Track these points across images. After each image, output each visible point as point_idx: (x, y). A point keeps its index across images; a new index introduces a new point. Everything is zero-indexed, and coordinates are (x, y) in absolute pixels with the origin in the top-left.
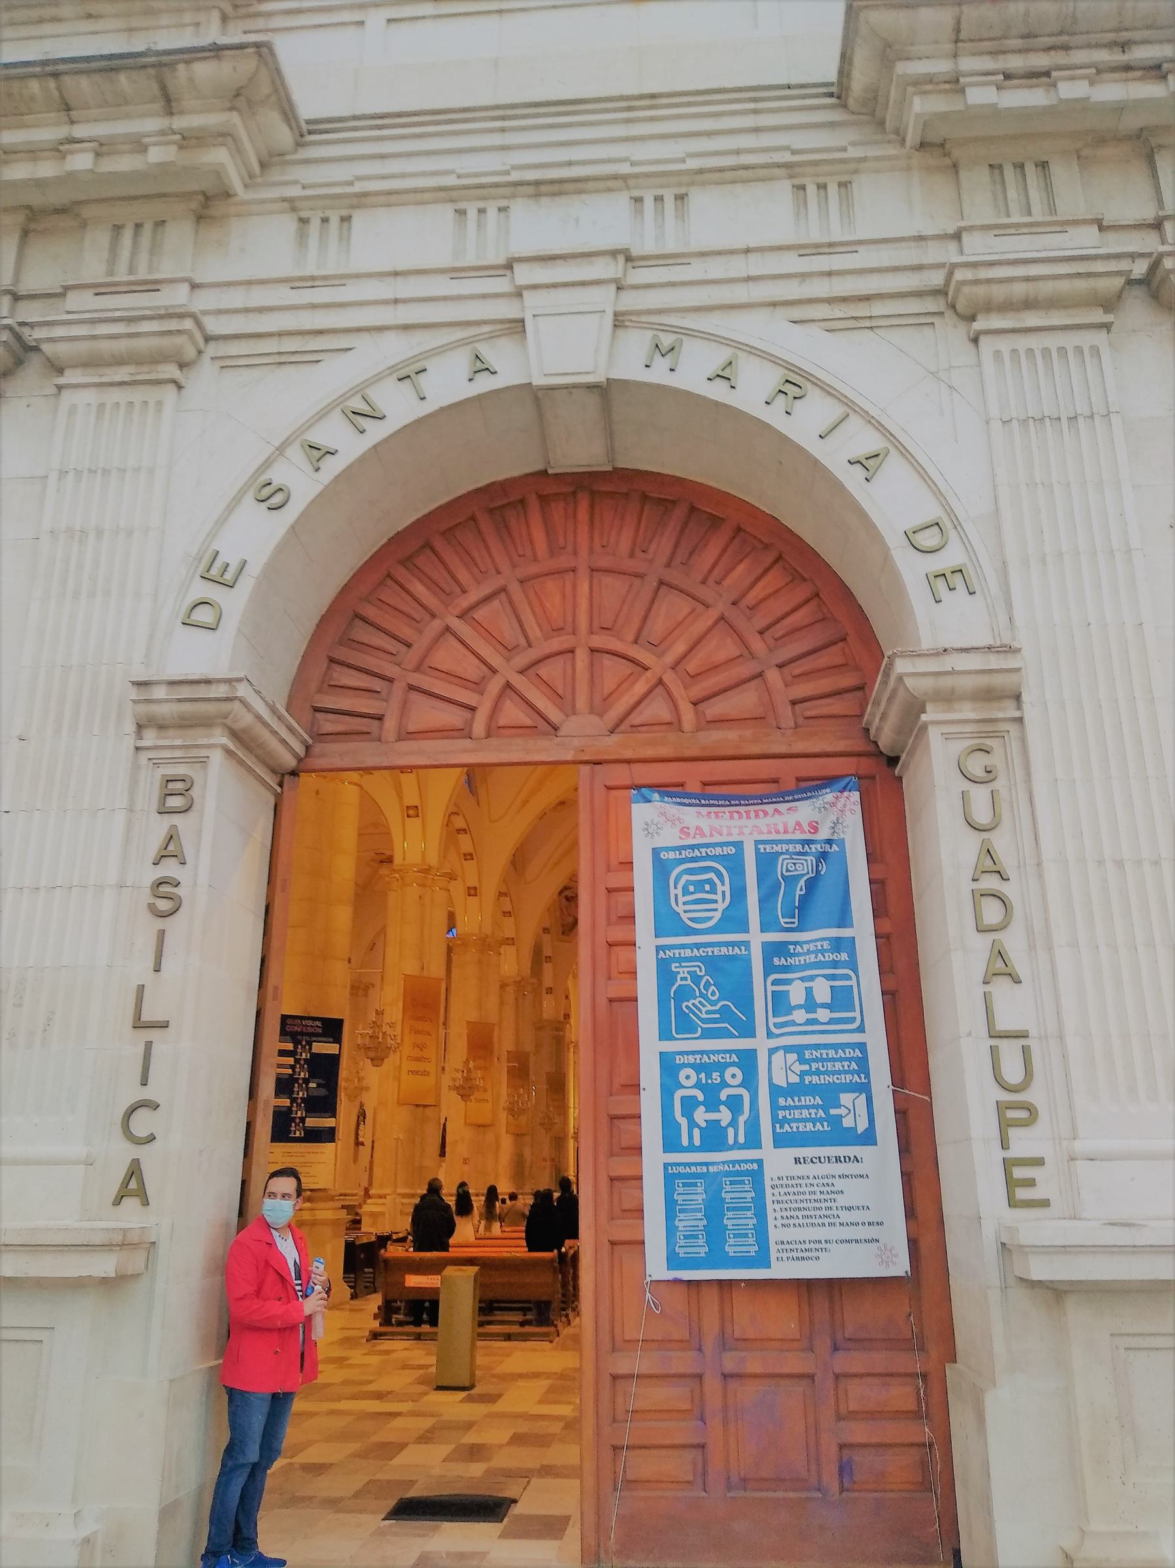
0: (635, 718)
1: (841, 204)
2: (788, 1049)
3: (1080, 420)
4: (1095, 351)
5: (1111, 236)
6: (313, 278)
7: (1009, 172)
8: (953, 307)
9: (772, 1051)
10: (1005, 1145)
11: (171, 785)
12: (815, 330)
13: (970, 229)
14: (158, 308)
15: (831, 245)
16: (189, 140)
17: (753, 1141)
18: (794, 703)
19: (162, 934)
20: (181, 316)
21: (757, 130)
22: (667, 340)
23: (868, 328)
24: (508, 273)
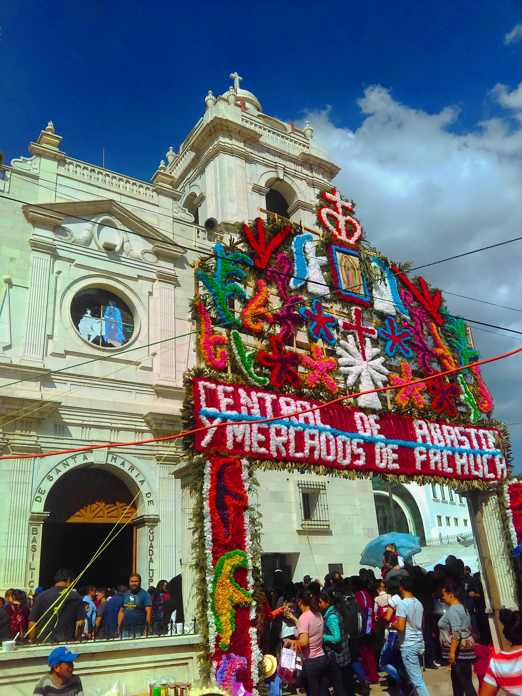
0: (97, 516)
10: (149, 585)
22: (115, 457)
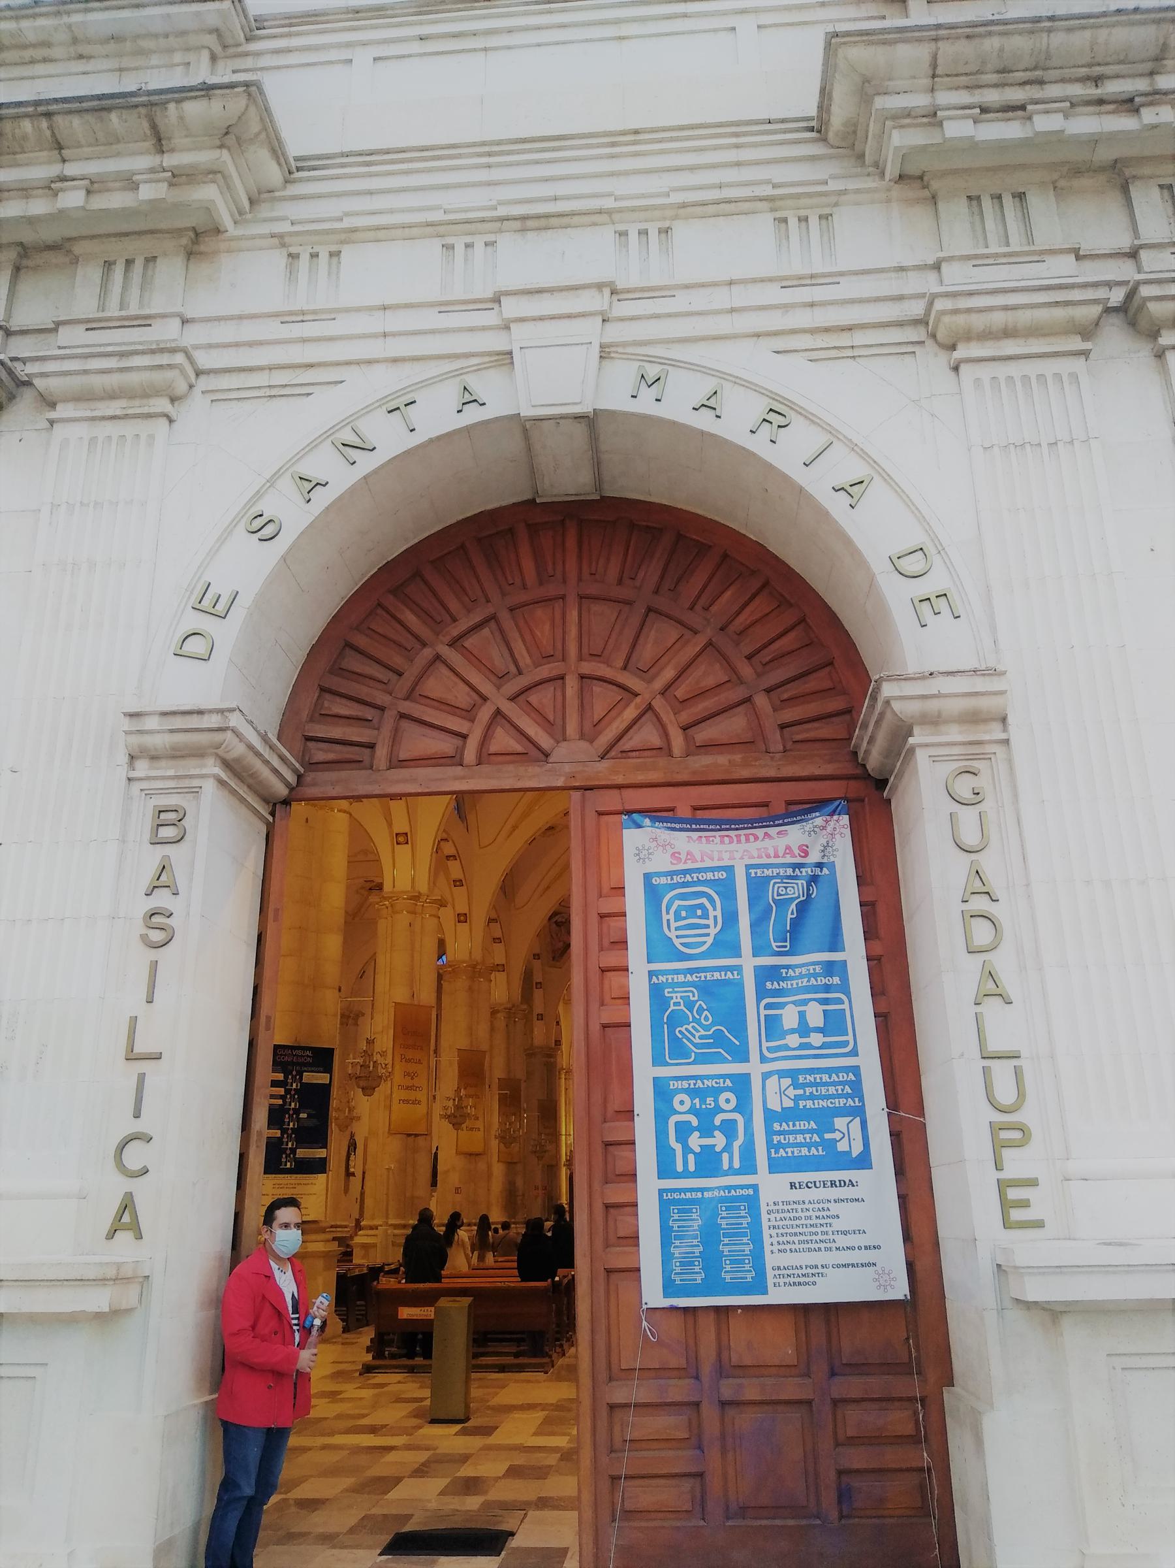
0: (627, 744)
1: (821, 236)
2: (782, 1074)
3: (1060, 445)
4: (1074, 377)
5: (1087, 265)
6: (303, 313)
7: (987, 203)
8: (933, 336)
9: (766, 1076)
10: (998, 1167)
11: (163, 816)
12: (798, 360)
13: (950, 259)
14: (151, 342)
15: (812, 277)
16: (178, 177)
17: (749, 1166)
18: (782, 727)
19: (154, 965)
20: (173, 351)
21: (738, 164)
22: (652, 372)
23: (851, 357)
24: (496, 306)
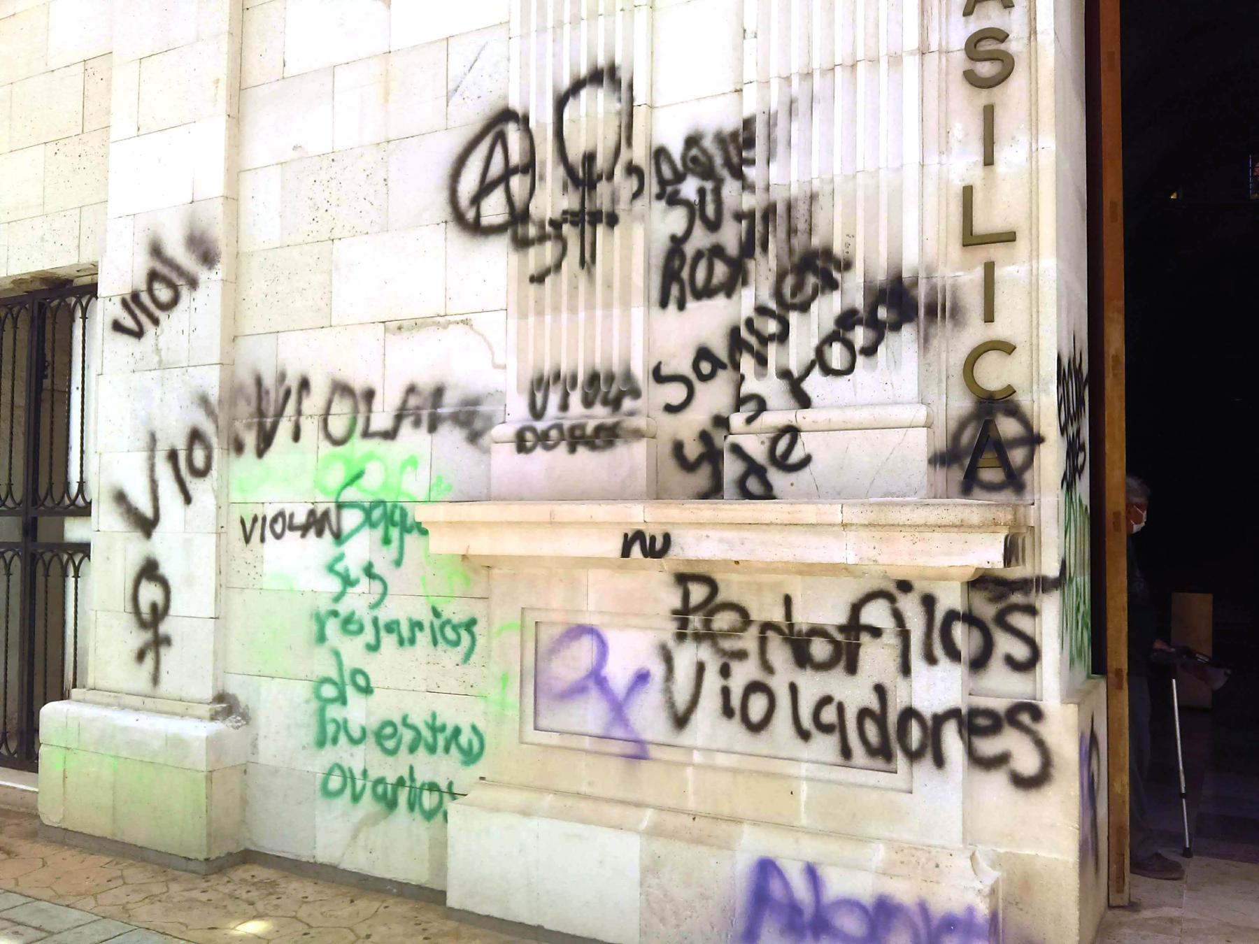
19: (989, 114)
